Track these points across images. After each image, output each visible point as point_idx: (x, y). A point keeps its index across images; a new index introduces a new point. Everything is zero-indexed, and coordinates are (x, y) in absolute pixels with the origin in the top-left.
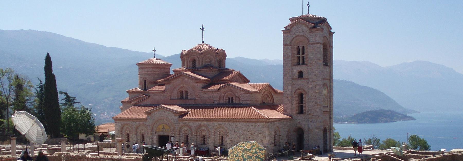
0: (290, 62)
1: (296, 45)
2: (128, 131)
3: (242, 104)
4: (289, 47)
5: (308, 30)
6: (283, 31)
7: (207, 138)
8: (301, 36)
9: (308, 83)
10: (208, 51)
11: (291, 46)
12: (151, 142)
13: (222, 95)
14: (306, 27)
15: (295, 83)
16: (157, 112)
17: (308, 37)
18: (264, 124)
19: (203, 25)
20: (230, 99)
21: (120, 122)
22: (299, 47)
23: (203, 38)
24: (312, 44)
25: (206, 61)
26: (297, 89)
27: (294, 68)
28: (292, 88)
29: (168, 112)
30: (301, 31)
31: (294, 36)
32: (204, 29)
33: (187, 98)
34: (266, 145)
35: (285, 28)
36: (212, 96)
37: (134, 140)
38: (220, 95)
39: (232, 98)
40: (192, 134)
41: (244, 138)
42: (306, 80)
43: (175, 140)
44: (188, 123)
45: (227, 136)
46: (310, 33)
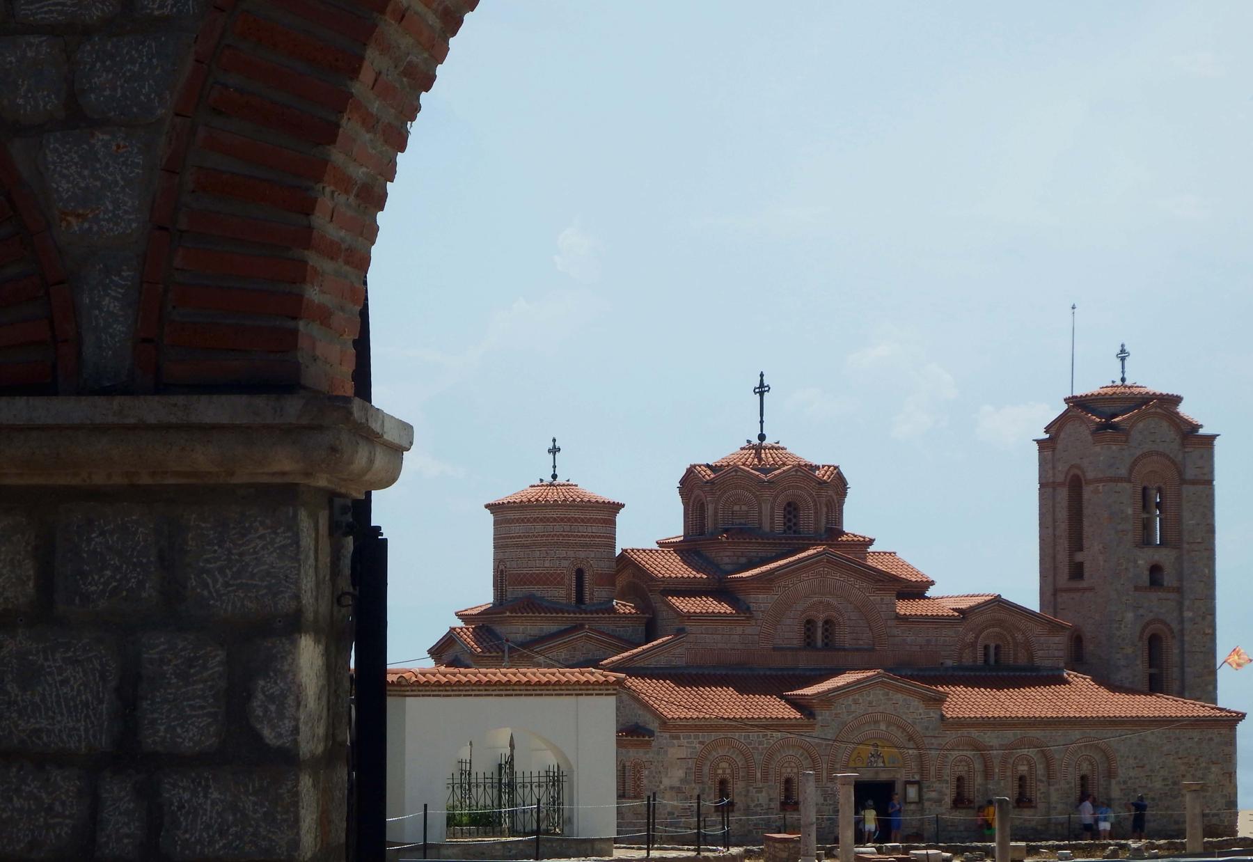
2: (724, 769)
3: (1037, 669)
7: (1038, 783)
8: (1158, 453)
11: (1131, 485)
12: (832, 807)
13: (970, 637)
16: (857, 697)
18: (1228, 732)
20: (992, 651)
21: (696, 737)
23: (762, 422)
24: (1194, 482)
26: (1148, 624)
29: (899, 697)
30: (1158, 441)
31: (1138, 453)
33: (829, 645)
34: (1232, 799)
36: (937, 640)
37: (756, 802)
40: (987, 773)
41: (1164, 780)
42: (1173, 596)
43: (926, 796)
44: (974, 733)
45: (1110, 774)
46: (1186, 450)
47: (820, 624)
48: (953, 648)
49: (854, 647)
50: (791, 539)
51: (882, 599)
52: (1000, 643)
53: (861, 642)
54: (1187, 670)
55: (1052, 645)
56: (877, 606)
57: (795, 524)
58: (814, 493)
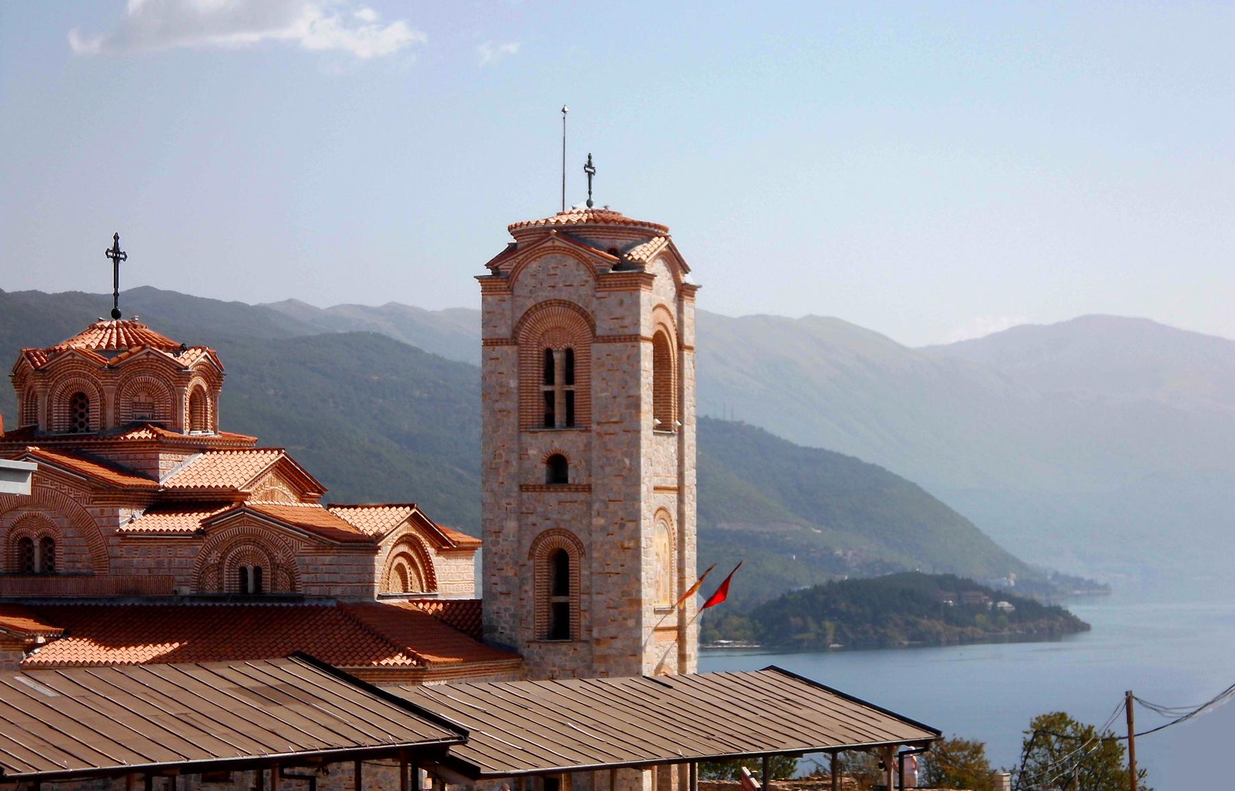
0: (513, 419)
1: (539, 344)
3: (301, 598)
4: (510, 352)
5: (589, 279)
6: (481, 279)
9: (589, 504)
10: (145, 357)
11: (516, 348)
13: (214, 558)
14: (582, 266)
15: (535, 508)
17: (589, 311)
19: (116, 237)
22: (549, 353)
25: (136, 399)
27: (529, 440)
28: (520, 527)
30: (561, 285)
31: (530, 303)
32: (111, 254)
33: (49, 569)
35: (488, 265)
36: (170, 563)
38: (205, 559)
39: (258, 571)
42: (581, 496)
46: (599, 295)
47: (36, 543)
48: (191, 571)
49: (71, 571)
50: (82, 438)
51: (102, 511)
52: (259, 564)
53: (79, 565)
54: (595, 597)
55: (321, 567)
56: (95, 520)
57: (87, 420)
58: (100, 381)
